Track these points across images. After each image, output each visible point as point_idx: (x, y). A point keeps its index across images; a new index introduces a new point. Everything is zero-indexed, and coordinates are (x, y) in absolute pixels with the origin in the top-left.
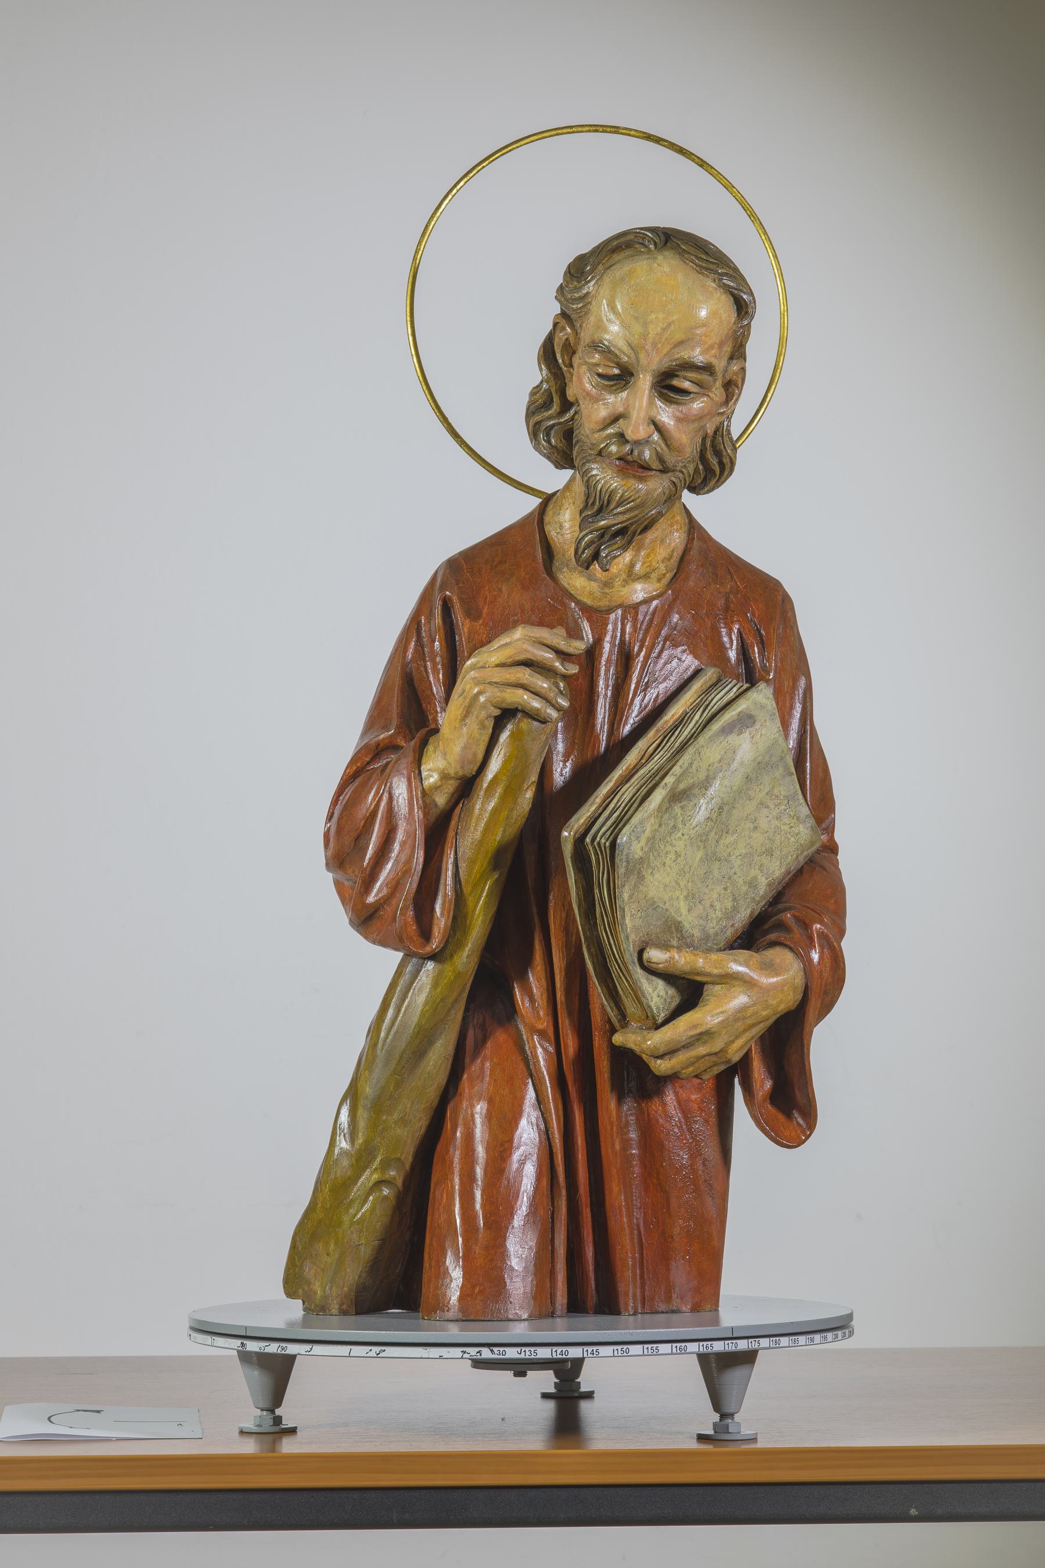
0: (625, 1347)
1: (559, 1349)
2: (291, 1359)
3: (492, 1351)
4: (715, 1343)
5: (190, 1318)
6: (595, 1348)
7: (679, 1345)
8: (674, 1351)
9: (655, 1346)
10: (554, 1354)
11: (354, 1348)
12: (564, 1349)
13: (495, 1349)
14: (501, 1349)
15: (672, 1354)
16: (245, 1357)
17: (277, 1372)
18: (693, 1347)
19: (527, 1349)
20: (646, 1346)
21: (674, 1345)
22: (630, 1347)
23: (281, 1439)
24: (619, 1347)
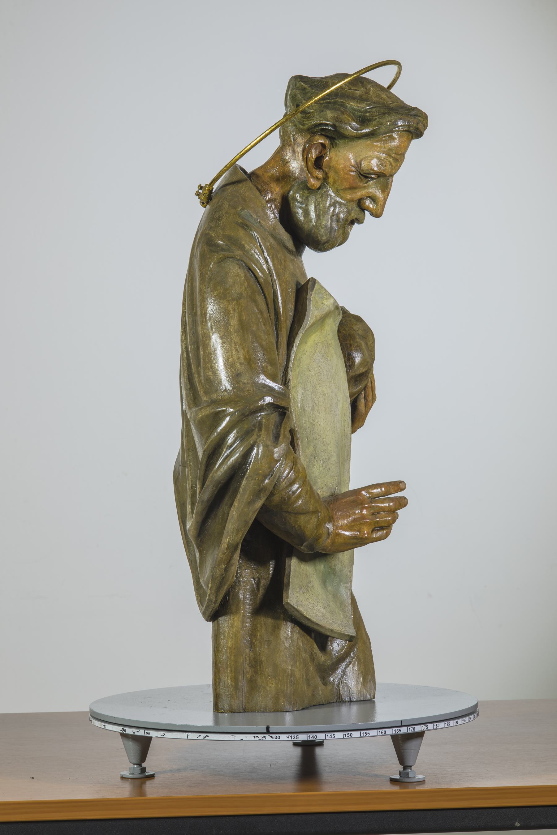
2: (150, 738)
5: (91, 710)
7: (381, 730)
15: (377, 736)
16: (124, 736)
17: (143, 745)
21: (379, 731)
23: (145, 783)
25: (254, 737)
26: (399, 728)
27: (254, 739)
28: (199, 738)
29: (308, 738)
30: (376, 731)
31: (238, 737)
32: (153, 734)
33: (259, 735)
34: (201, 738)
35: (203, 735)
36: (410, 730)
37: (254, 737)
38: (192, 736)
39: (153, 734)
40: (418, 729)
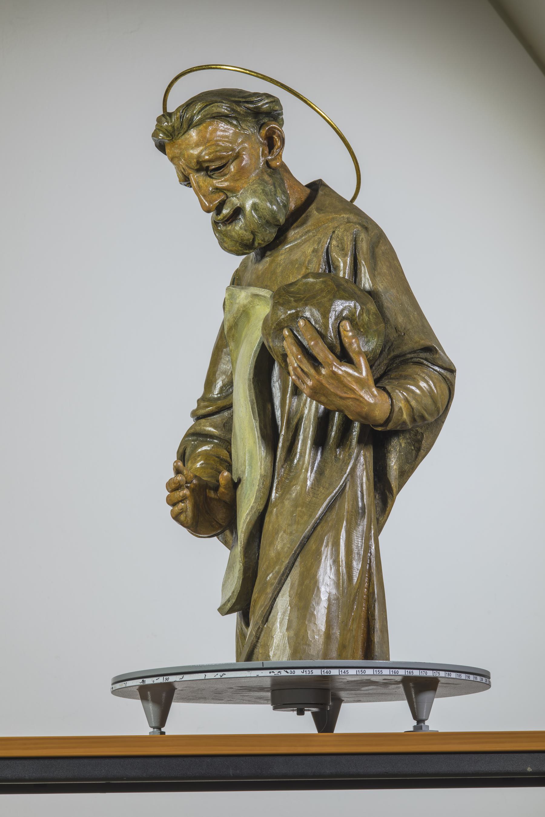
0: (363, 670)
1: (325, 670)
3: (286, 672)
4: (414, 671)
6: (346, 670)
8: (391, 673)
9: (380, 670)
10: (323, 673)
11: (206, 674)
12: (328, 670)
13: (289, 671)
14: (292, 670)
18: (402, 672)
19: (307, 670)
20: (375, 670)
22: (366, 670)
24: (360, 670)
25: (270, 673)
26: (411, 670)
27: (269, 675)
28: (217, 677)
29: (323, 673)
30: (389, 670)
31: (254, 673)
32: (172, 679)
33: (274, 671)
34: (218, 676)
35: (220, 674)
36: (423, 674)
37: (270, 673)
38: (210, 676)
39: (172, 679)
40: (430, 674)
